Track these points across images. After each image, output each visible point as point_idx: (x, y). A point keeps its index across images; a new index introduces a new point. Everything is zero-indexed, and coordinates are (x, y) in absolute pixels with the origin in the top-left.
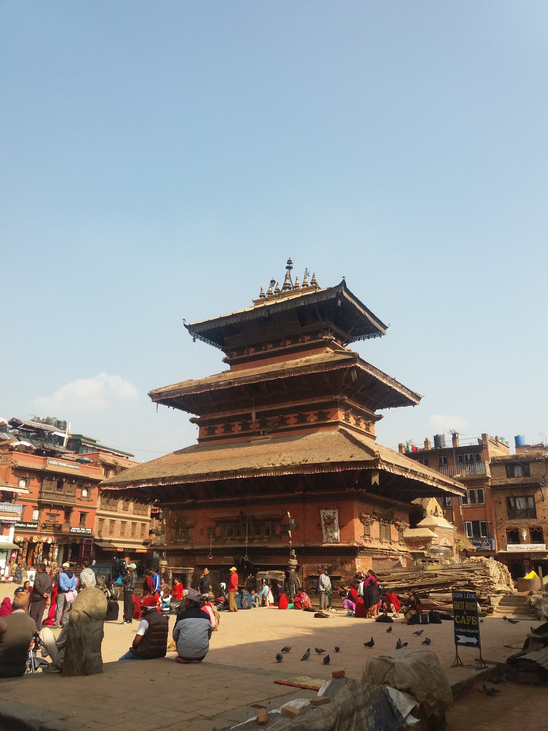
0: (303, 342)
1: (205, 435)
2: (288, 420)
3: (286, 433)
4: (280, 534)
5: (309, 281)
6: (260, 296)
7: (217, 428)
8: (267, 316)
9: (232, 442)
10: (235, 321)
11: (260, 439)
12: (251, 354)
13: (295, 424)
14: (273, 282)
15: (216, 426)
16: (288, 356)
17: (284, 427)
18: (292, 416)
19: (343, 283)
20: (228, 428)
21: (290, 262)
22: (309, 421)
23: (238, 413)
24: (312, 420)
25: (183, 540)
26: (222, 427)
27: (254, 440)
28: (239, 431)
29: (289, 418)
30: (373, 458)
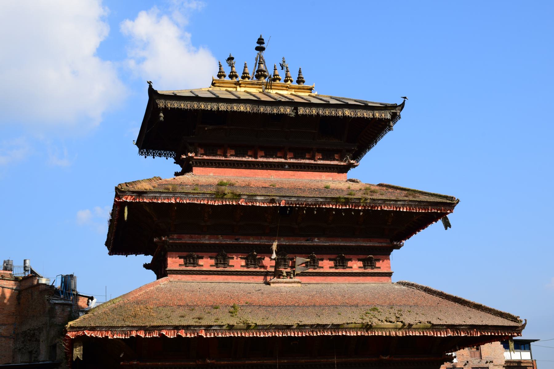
0: (313, 158)
2: (320, 262)
3: (318, 278)
5: (295, 78)
6: (219, 76)
8: (293, 114)
9: (230, 280)
11: (286, 283)
13: (331, 268)
14: (231, 59)
19: (402, 106)
21: (261, 41)
22: (351, 267)
27: (278, 283)
28: (242, 266)
30: (519, 325)
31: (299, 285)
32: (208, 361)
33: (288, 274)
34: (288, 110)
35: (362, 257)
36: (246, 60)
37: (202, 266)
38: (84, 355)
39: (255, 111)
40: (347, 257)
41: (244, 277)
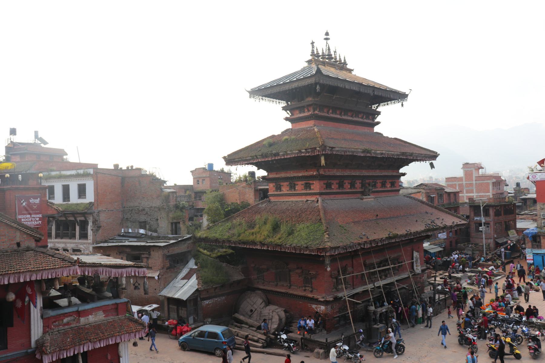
0: (362, 118)
6: (311, 55)
9: (344, 198)
15: (332, 182)
16: (354, 126)
17: (376, 190)
20: (341, 185)
21: (327, 34)
23: (347, 173)
24: (388, 186)
31: (373, 199)
34: (370, 92)
35: (390, 181)
41: (350, 195)
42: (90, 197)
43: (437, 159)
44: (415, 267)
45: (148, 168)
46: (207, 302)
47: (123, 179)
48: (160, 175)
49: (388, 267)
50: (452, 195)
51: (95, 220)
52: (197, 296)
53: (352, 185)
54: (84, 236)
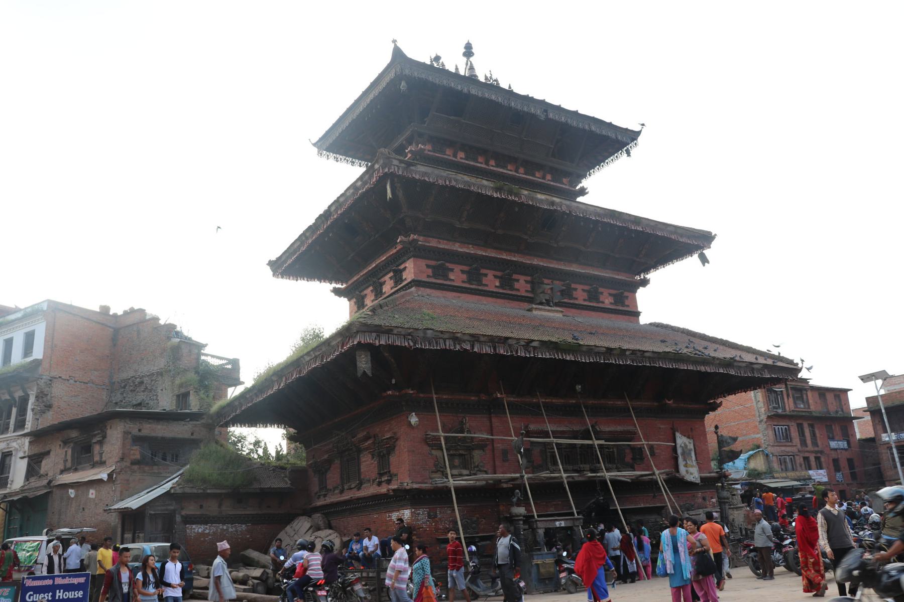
0: (544, 178)
1: (428, 276)
4: (631, 461)
7: (452, 270)
8: (543, 117)
10: (493, 97)
11: (549, 311)
12: (458, 159)
13: (585, 300)
17: (572, 301)
18: (580, 287)
20: (474, 276)
22: (603, 302)
24: (607, 301)
25: (465, 472)
26: (463, 272)
28: (496, 287)
29: (576, 289)
32: (499, 395)
33: (548, 303)
36: (454, 62)
37: (453, 280)
38: (373, 368)
39: (506, 103)
40: (601, 290)
42: (38, 353)
43: (713, 244)
44: (682, 469)
45: (165, 312)
46: (199, 529)
47: (116, 331)
48: (192, 330)
49: (589, 442)
50: (830, 397)
51: (42, 392)
52: (174, 511)
53: (507, 282)
54: (20, 424)
